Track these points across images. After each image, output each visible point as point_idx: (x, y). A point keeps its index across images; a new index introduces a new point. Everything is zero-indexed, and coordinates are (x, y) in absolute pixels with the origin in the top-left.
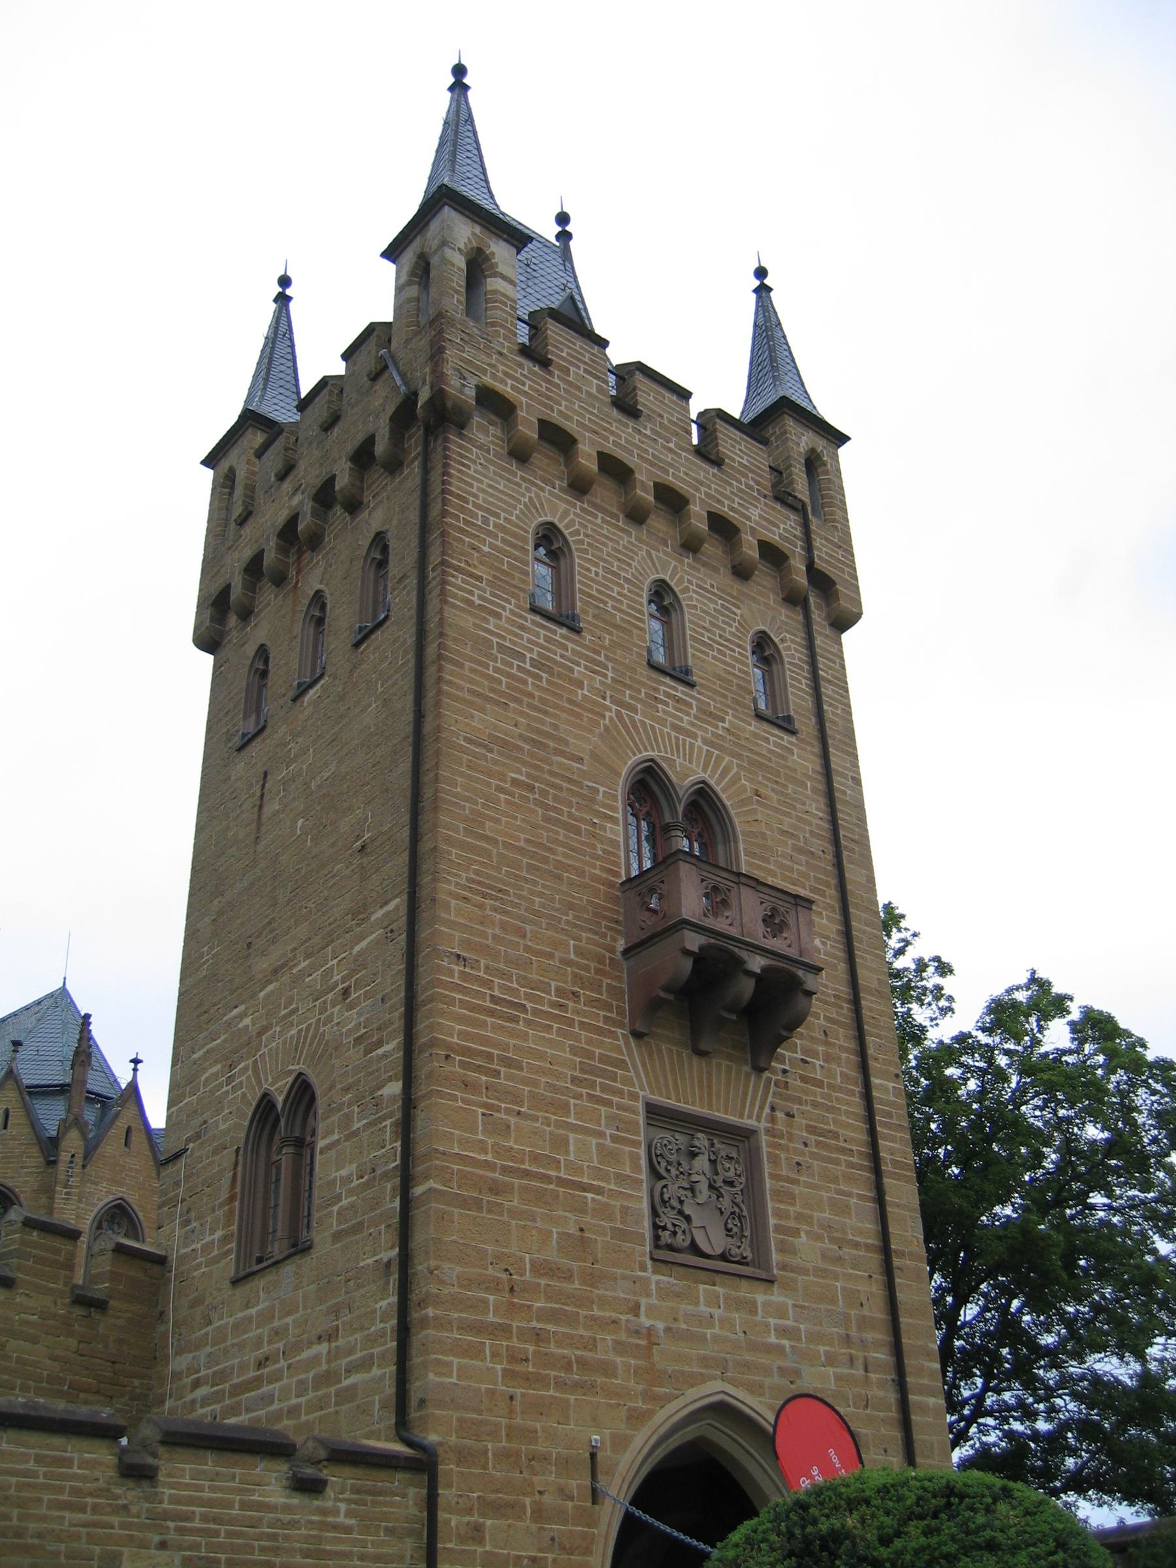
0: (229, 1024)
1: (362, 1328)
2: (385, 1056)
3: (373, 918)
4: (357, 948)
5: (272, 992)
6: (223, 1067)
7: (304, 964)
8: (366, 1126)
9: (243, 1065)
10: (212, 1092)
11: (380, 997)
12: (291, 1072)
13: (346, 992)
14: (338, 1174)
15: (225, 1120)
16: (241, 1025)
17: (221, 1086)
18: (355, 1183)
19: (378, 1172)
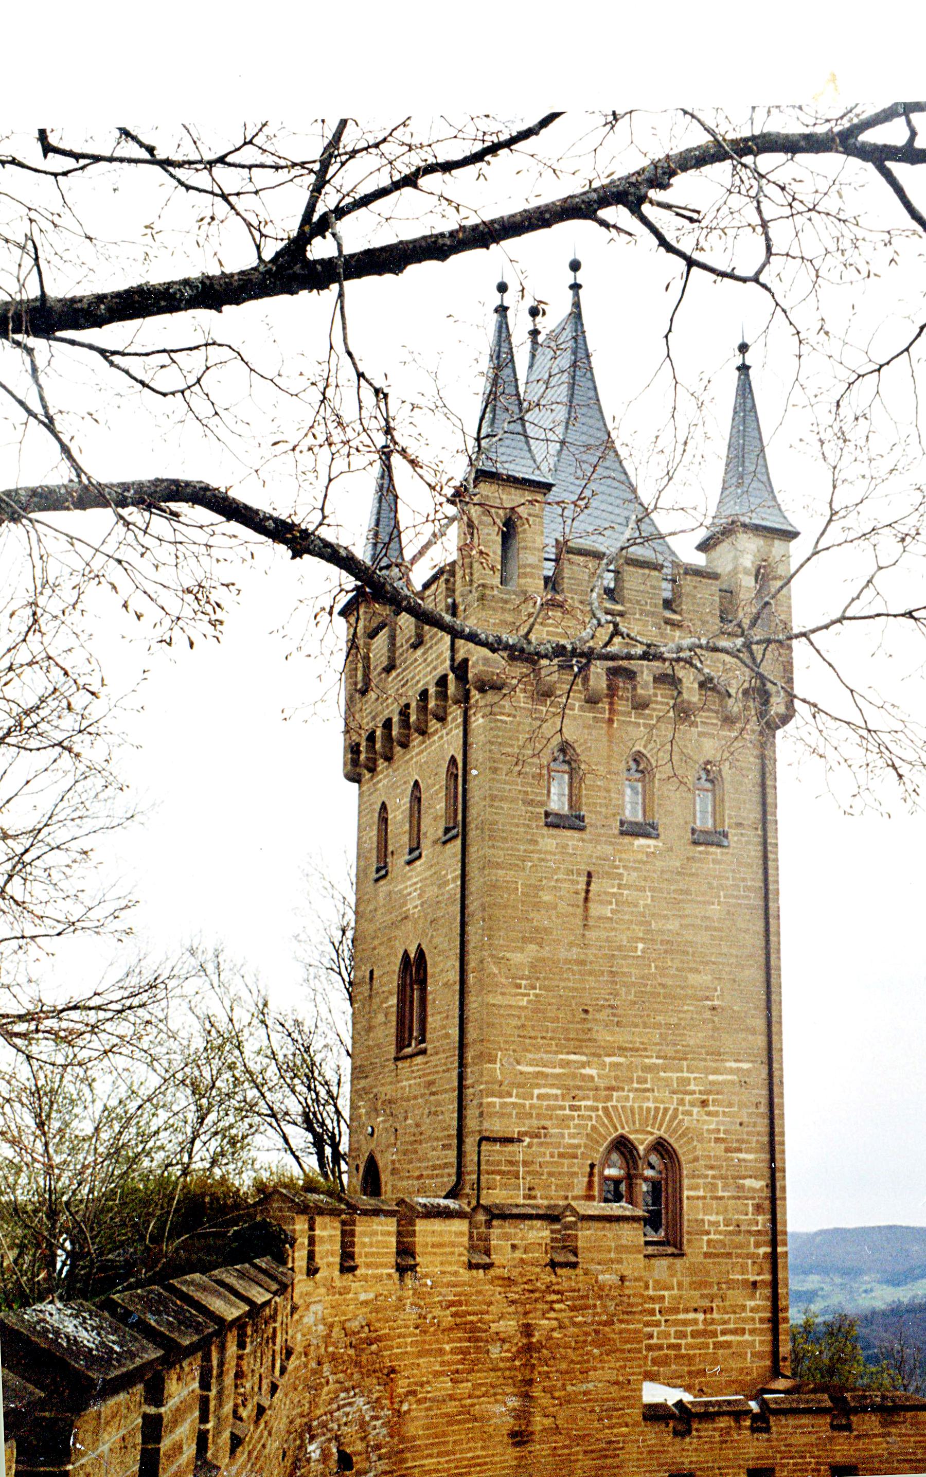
0: (565, 1064)
1: (735, 1312)
2: (744, 1160)
3: (728, 1064)
4: (711, 1078)
5: (621, 1064)
6: (563, 1095)
7: (654, 1060)
8: (729, 1198)
9: (589, 1103)
10: (549, 1108)
11: (739, 1121)
12: (652, 1134)
13: (704, 1103)
14: (706, 1218)
15: (571, 1136)
16: (583, 1071)
17: (562, 1108)
18: (722, 1228)
19: (743, 1228)
